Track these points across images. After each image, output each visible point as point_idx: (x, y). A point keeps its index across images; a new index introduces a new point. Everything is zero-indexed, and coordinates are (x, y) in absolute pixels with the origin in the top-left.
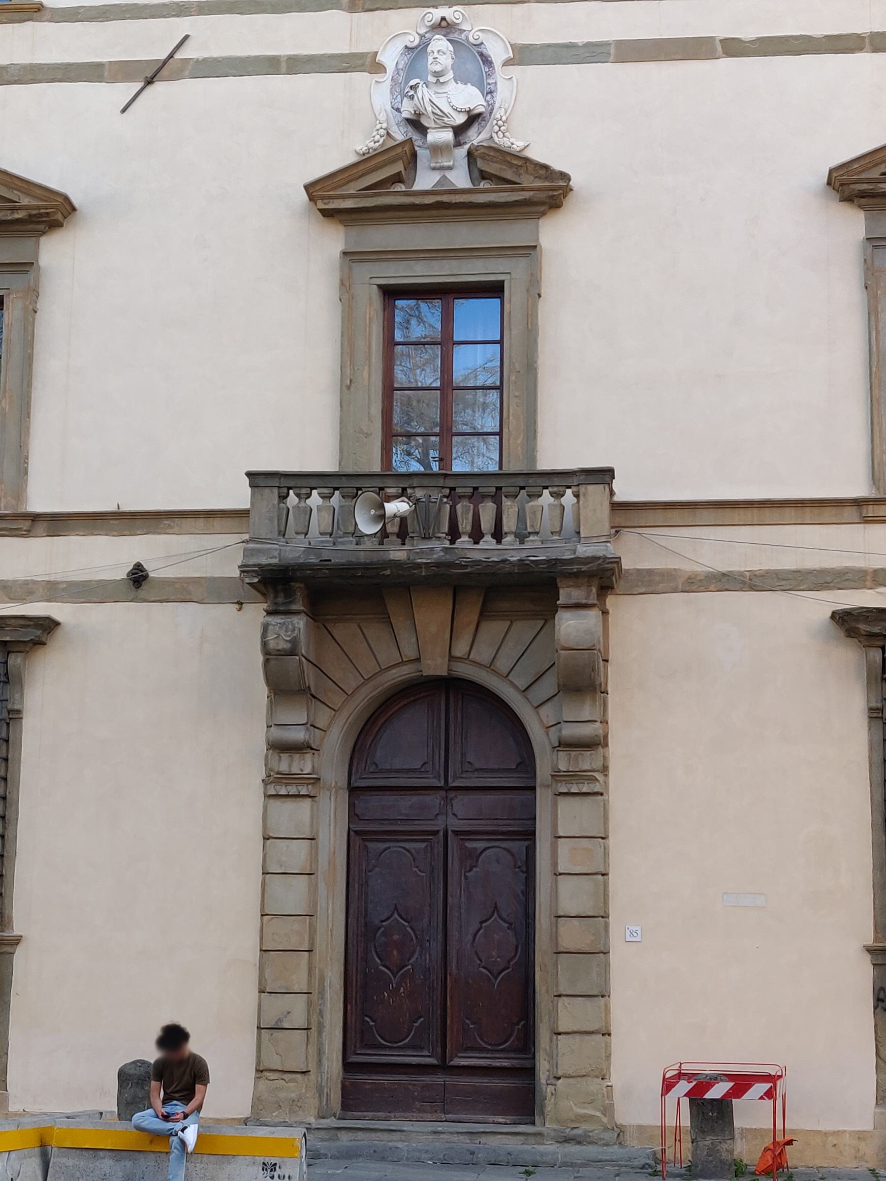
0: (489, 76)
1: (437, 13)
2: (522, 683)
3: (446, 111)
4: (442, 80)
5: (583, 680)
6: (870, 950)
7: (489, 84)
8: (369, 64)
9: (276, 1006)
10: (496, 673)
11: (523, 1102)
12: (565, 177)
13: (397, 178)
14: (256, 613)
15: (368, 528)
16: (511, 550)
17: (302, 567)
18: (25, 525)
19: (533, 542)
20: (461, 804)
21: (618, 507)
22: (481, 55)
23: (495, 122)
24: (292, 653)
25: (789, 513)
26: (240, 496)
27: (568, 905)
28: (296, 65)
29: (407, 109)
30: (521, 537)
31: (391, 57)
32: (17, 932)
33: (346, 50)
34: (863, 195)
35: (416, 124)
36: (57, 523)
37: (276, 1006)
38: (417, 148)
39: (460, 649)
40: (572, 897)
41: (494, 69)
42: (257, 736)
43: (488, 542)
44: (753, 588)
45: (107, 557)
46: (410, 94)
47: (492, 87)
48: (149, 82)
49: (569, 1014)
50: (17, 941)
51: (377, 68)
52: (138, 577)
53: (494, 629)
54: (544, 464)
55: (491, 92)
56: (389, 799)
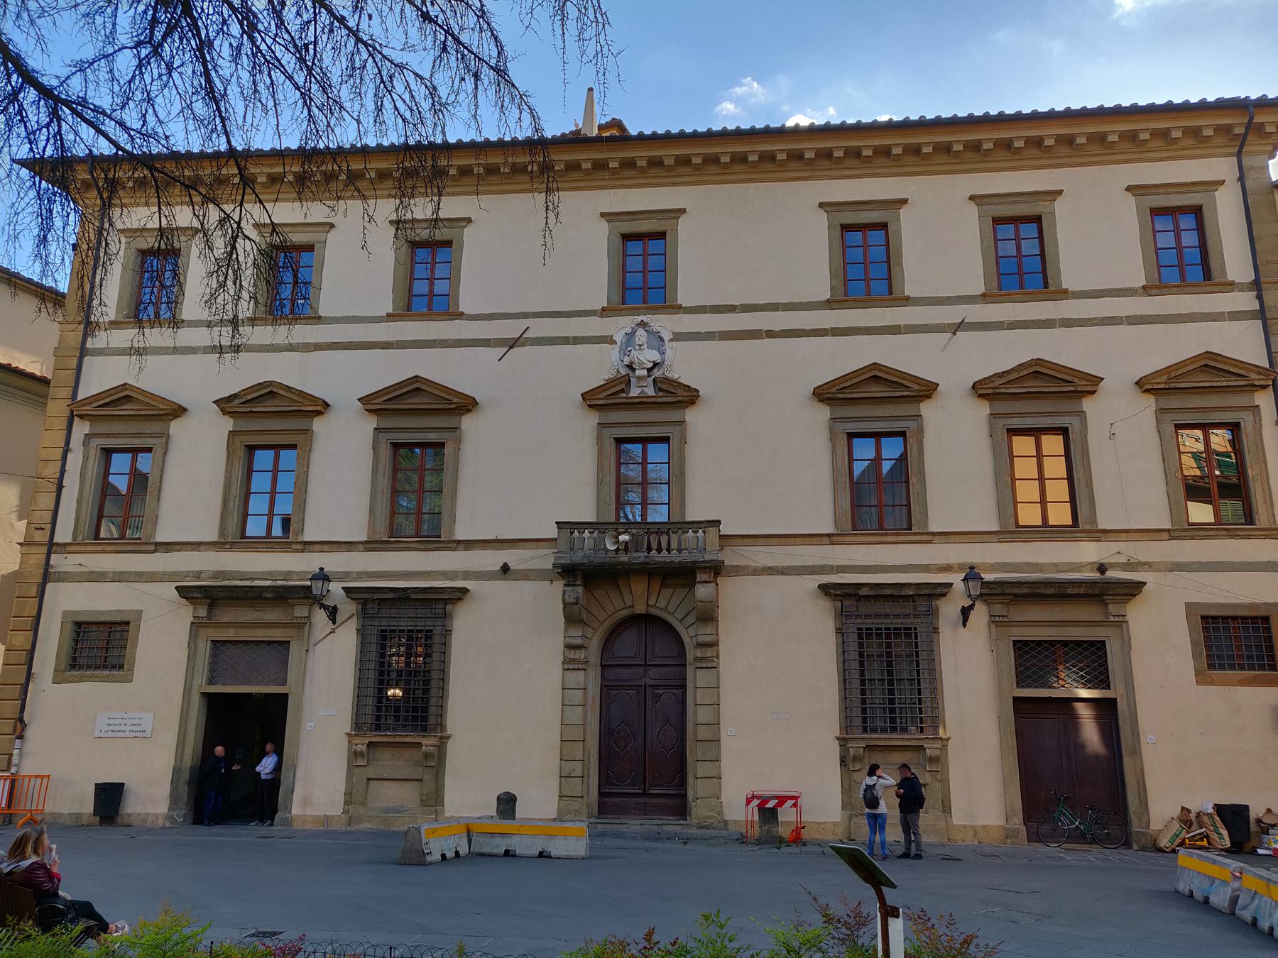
2: (680, 617)
5: (708, 616)
6: (838, 739)
8: (609, 340)
9: (568, 766)
11: (682, 811)
13: (622, 391)
14: (559, 586)
15: (611, 547)
16: (675, 557)
17: (581, 564)
18: (454, 545)
19: (685, 553)
20: (652, 672)
21: (721, 536)
24: (576, 604)
25: (798, 539)
26: (553, 532)
27: (701, 719)
28: (577, 340)
29: (627, 360)
30: (680, 551)
31: (619, 338)
34: (829, 399)
35: (630, 367)
36: (468, 544)
37: (568, 766)
39: (651, 603)
40: (703, 715)
42: (560, 642)
43: (664, 553)
44: (783, 574)
45: (492, 560)
48: (511, 347)
49: (702, 769)
50: (449, 737)
52: (505, 569)
53: (667, 592)
54: (688, 519)
56: (619, 670)
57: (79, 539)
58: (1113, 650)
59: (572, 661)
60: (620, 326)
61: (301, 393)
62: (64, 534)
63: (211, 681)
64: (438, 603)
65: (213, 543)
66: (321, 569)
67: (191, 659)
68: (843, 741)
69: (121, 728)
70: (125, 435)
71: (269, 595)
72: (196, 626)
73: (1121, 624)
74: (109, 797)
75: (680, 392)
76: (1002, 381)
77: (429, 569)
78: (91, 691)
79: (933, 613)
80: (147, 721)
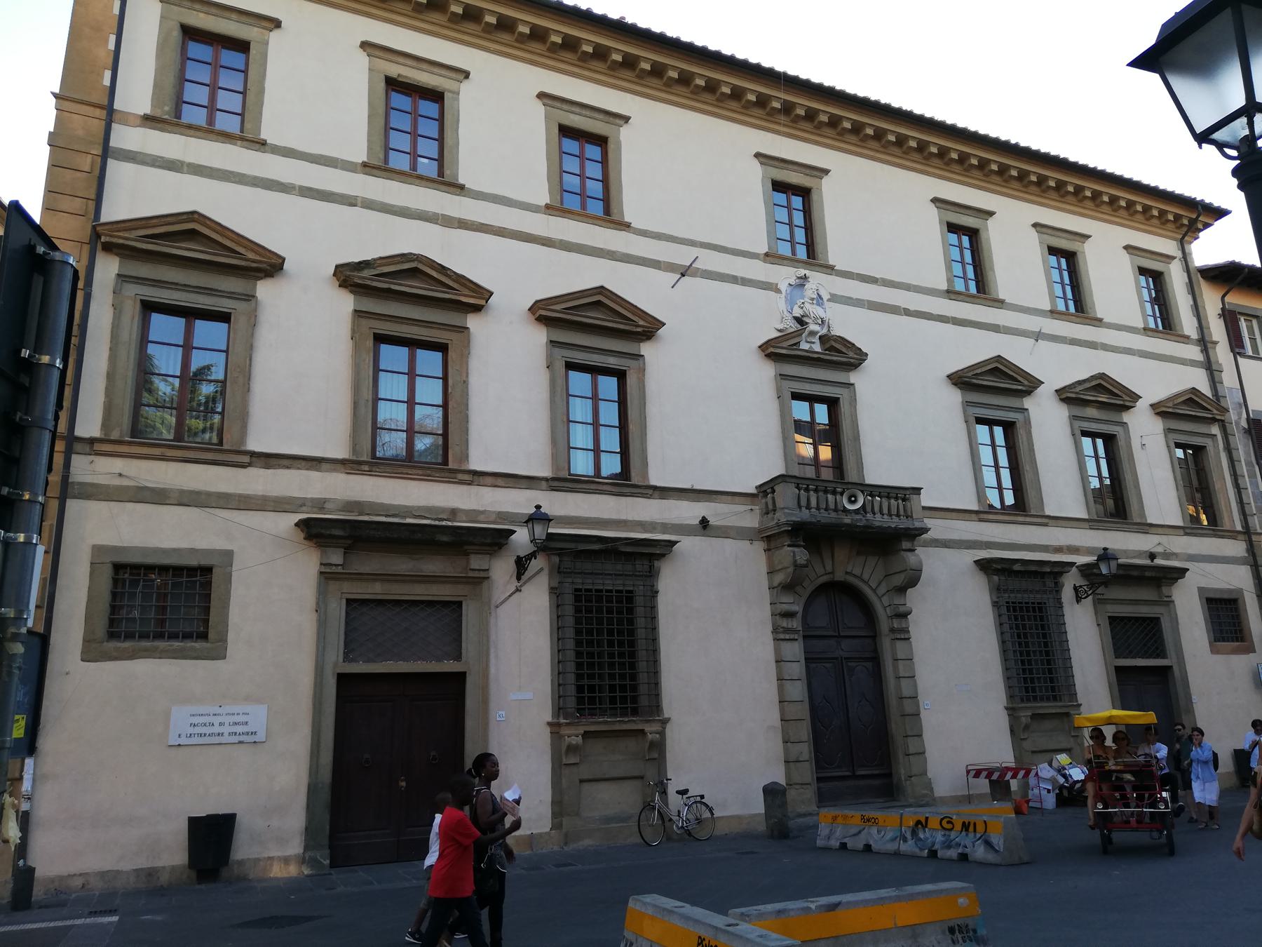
6: (1007, 708)
8: (774, 288)
9: (795, 750)
10: (863, 581)
18: (650, 492)
28: (745, 282)
29: (797, 312)
32: (666, 716)
43: (878, 516)
45: (689, 512)
48: (683, 275)
51: (778, 291)
52: (704, 522)
57: (115, 435)
58: (1165, 624)
59: (787, 630)
61: (461, 279)
62: (89, 424)
63: (348, 655)
64: (645, 556)
65: (343, 462)
66: (538, 507)
67: (322, 625)
68: (1011, 711)
69: (216, 729)
70: (185, 288)
71: (445, 539)
72: (327, 576)
73: (1169, 603)
74: (212, 836)
75: (851, 354)
76: (1081, 388)
77: (623, 517)
78: (152, 674)
79: (1058, 588)
80: (257, 718)
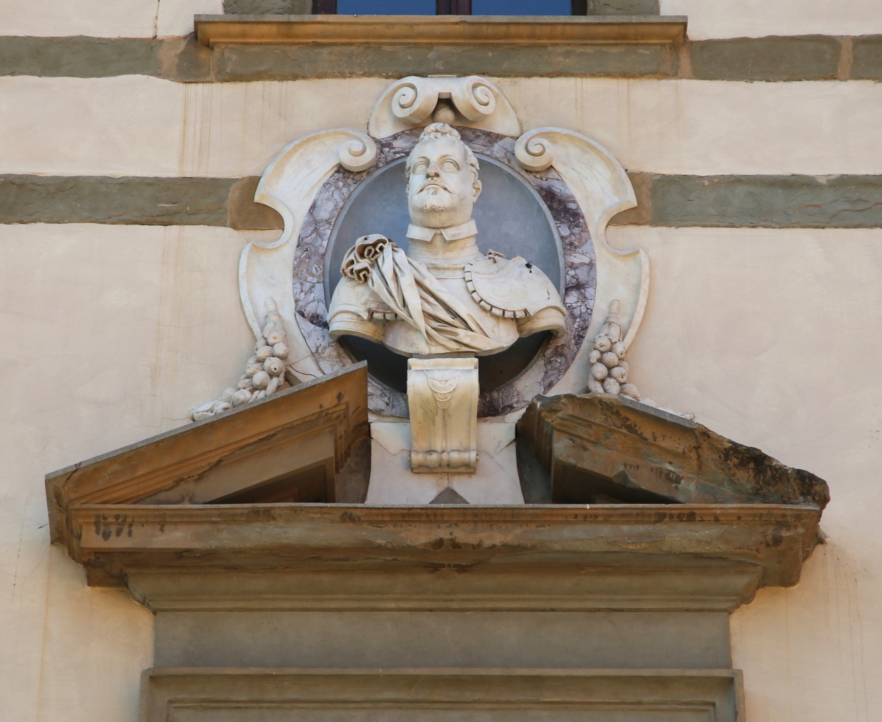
0: (570, 246)
1: (430, 88)
3: (463, 311)
4: (448, 234)
7: (572, 266)
12: (812, 489)
22: (549, 196)
23: (595, 355)
29: (349, 307)
31: (296, 188)
33: (168, 168)
38: (371, 418)
41: (585, 229)
46: (356, 267)
47: (582, 275)
55: (579, 286)
60: (301, 135)
